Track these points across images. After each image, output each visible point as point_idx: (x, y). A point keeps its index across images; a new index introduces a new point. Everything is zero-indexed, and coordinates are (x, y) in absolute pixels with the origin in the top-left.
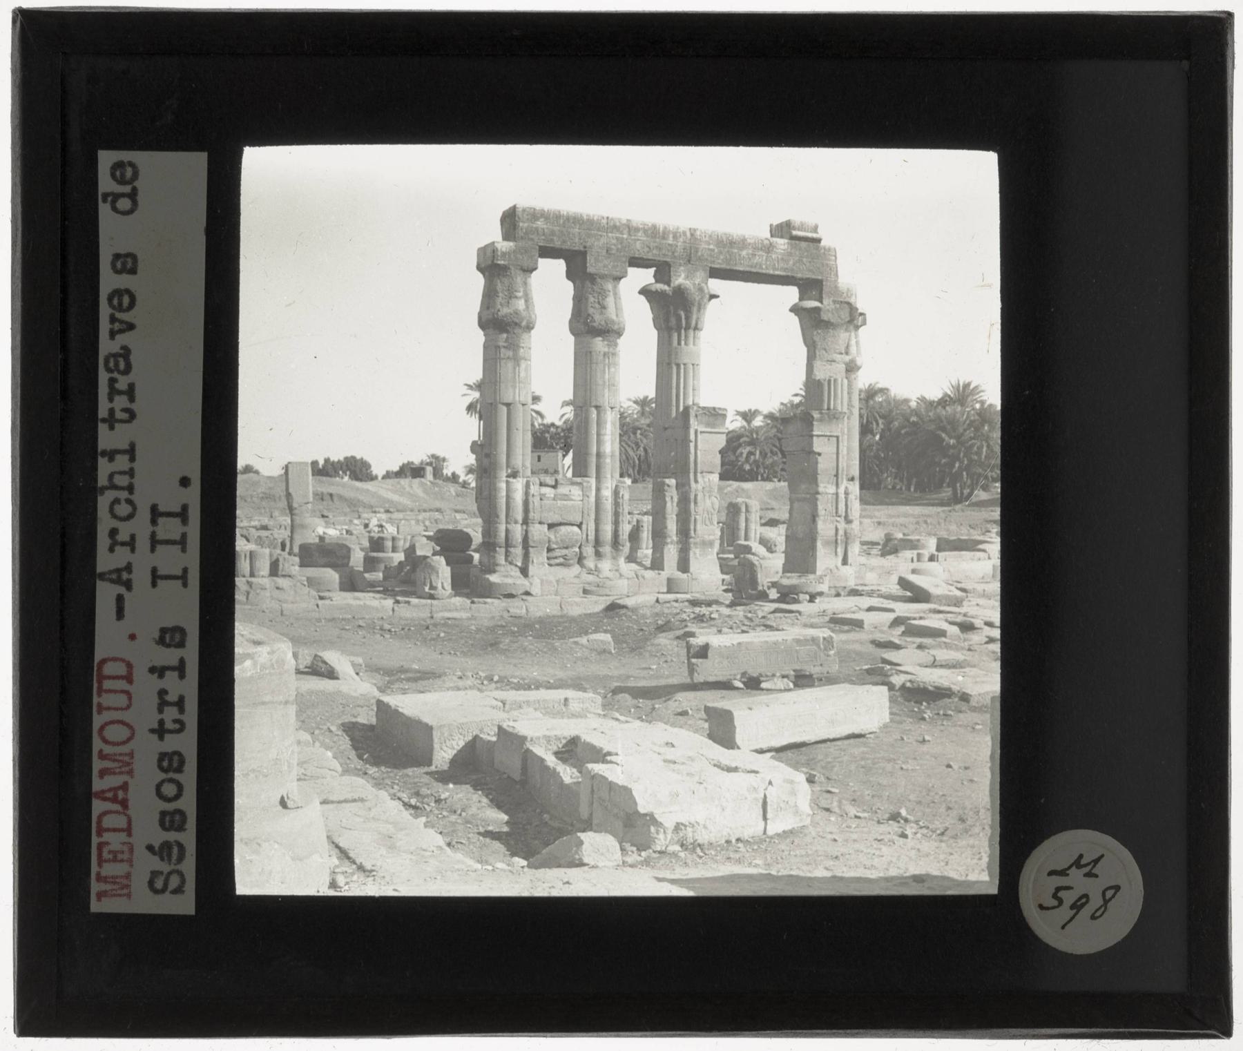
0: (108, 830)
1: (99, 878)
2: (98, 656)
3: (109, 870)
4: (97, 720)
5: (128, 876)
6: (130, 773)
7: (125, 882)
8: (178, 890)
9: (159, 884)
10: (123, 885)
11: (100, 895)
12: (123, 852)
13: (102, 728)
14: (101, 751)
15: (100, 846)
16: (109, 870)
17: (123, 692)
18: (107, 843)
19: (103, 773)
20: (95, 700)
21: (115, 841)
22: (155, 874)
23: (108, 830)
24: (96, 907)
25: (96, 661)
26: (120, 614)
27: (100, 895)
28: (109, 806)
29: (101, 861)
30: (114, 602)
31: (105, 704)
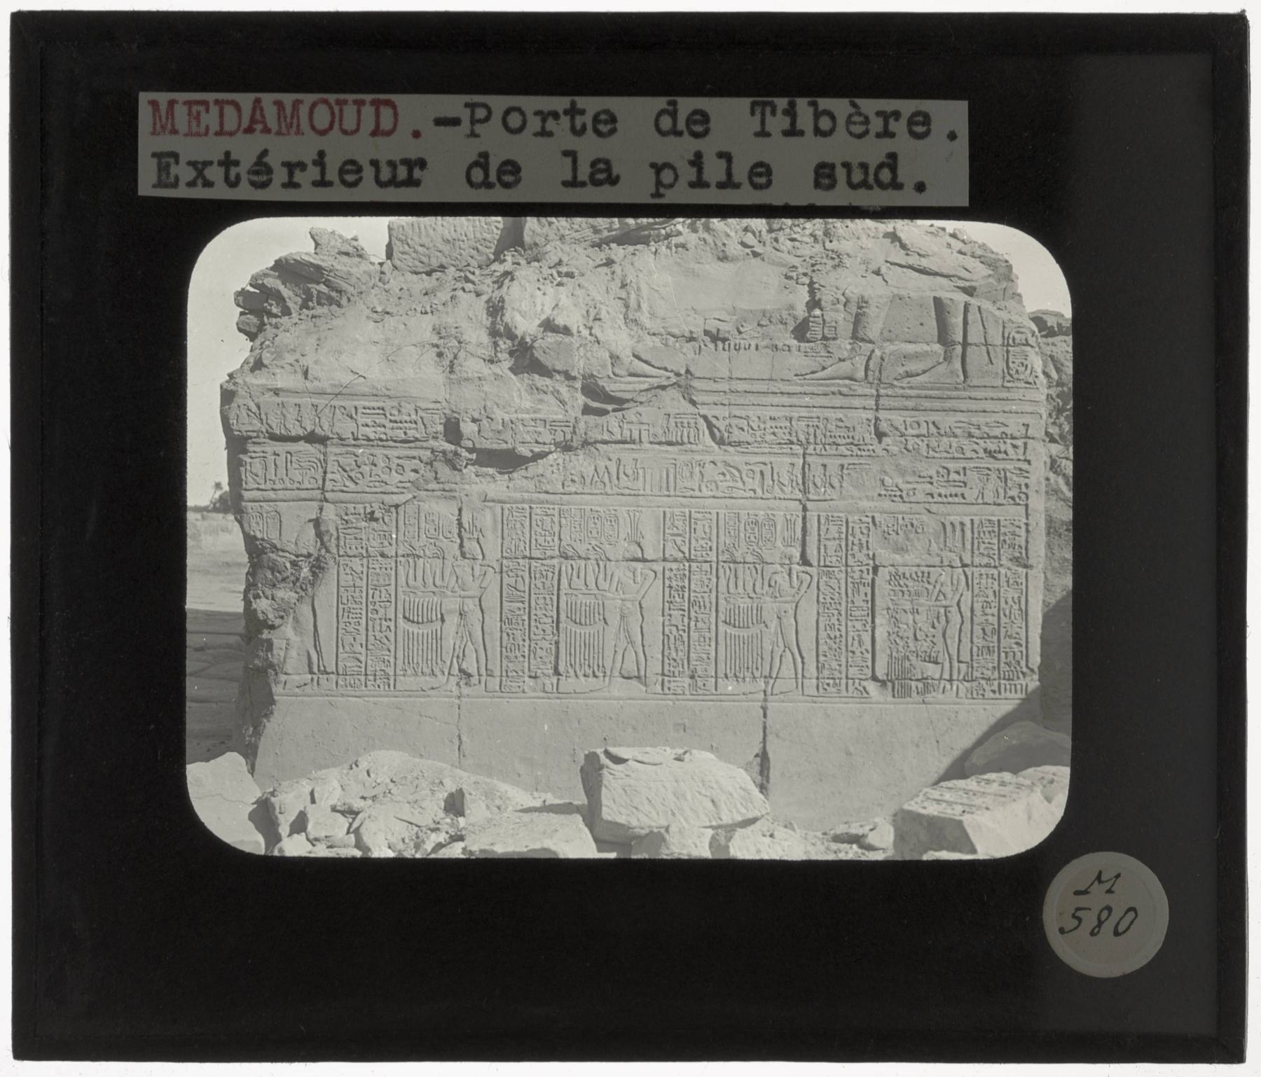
6: (279, 133)
19: (279, 104)
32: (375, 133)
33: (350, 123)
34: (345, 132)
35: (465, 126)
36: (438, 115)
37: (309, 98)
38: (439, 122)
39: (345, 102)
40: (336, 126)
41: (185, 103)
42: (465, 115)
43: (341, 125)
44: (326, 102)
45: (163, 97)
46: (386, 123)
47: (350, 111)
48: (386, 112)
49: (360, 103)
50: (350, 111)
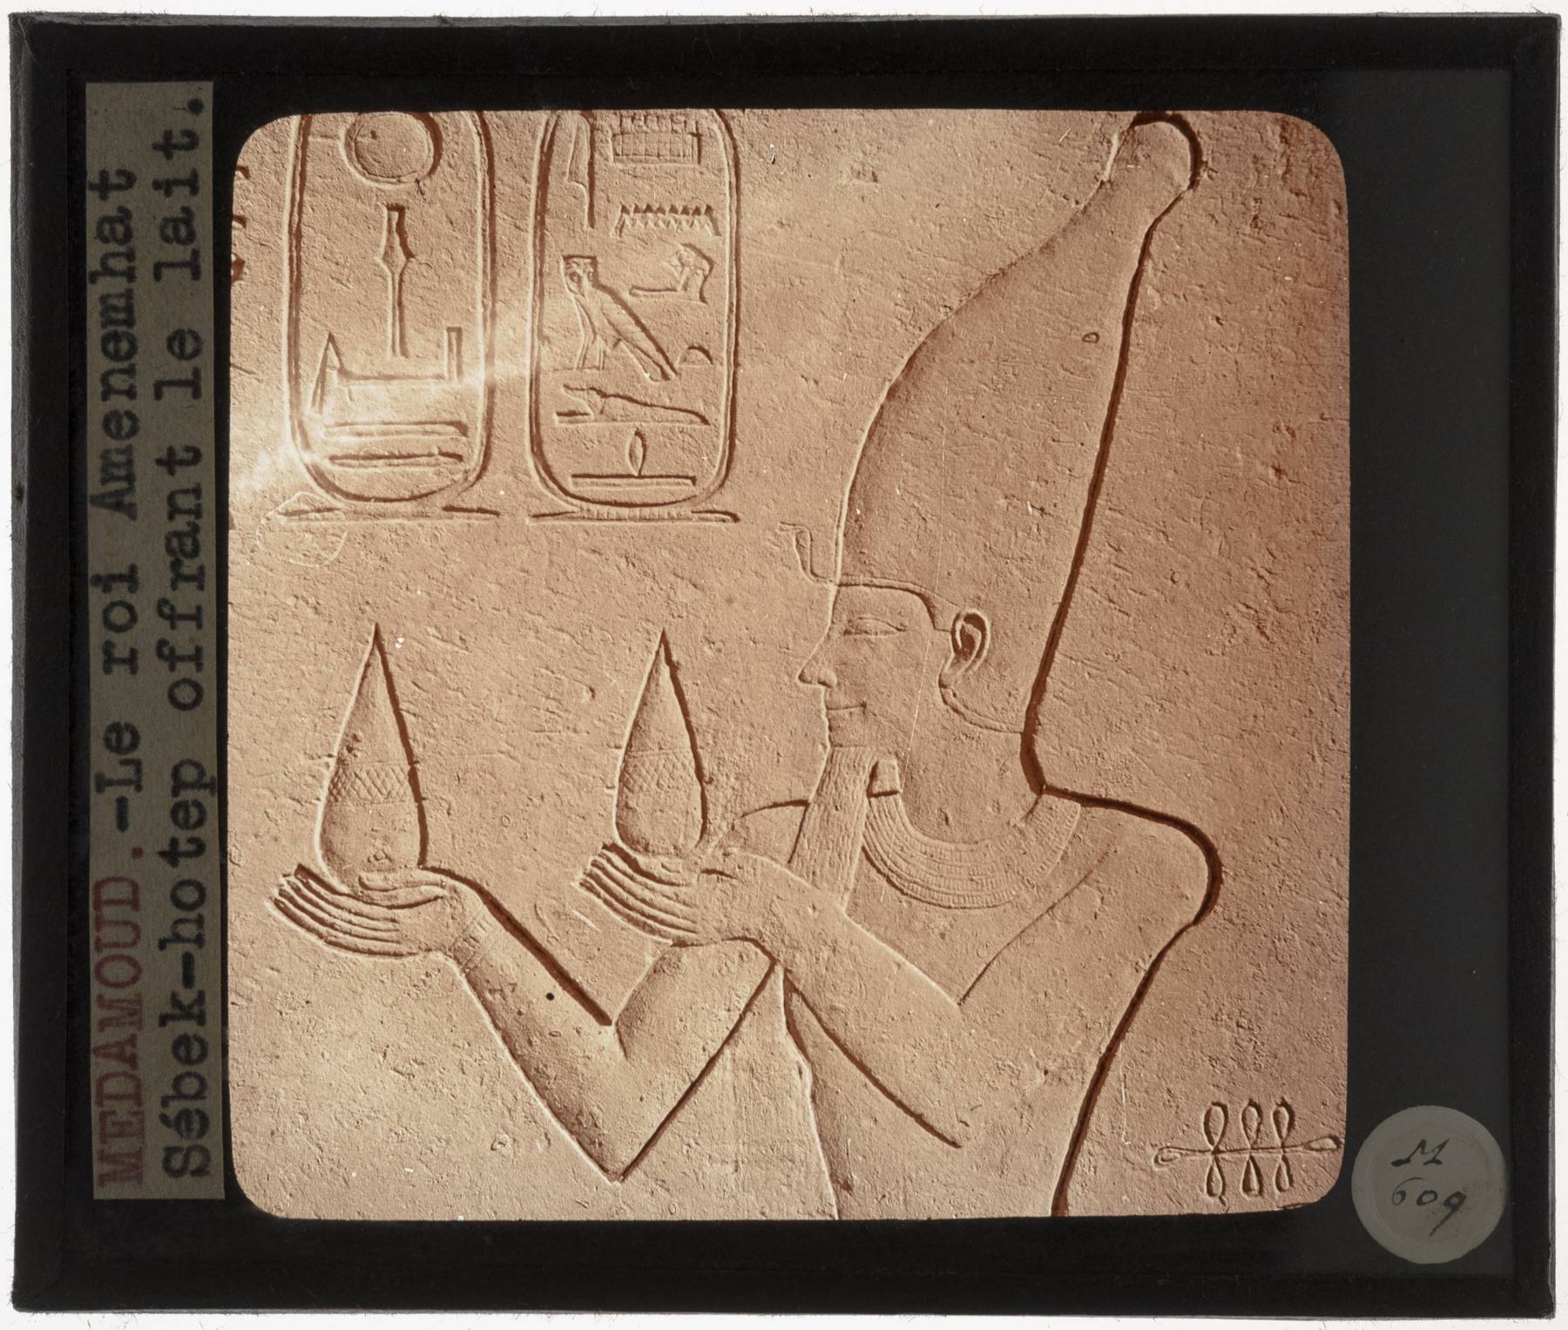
0: (110, 1097)
1: (103, 1157)
2: (98, 870)
3: (118, 1146)
4: (94, 958)
5: (139, 1155)
7: (133, 1160)
8: (200, 1172)
9: (177, 1162)
10: (134, 1168)
11: (103, 1179)
12: (130, 1123)
13: (100, 965)
14: (100, 998)
15: (103, 1116)
16: (118, 1146)
17: (126, 923)
18: (114, 1113)
20: (93, 934)
21: (123, 1109)
22: (170, 1151)
23: (110, 1097)
24: (100, 1193)
25: (91, 886)
26: (122, 824)
27: (103, 1179)
28: (114, 1065)
29: (103, 1140)
30: (114, 805)
31: (105, 940)
32: (135, 904)
33: (126, 935)
34: (134, 944)
35: (128, 792)
36: (115, 824)
37: (96, 988)
38: (122, 824)
39: (98, 941)
40: (125, 952)
41: (103, 1141)
42: (112, 793)
43: (125, 945)
44: (100, 965)
45: (98, 1168)
46: (124, 891)
47: (109, 934)
48: (109, 892)
49: (100, 923)
50: (109, 934)
